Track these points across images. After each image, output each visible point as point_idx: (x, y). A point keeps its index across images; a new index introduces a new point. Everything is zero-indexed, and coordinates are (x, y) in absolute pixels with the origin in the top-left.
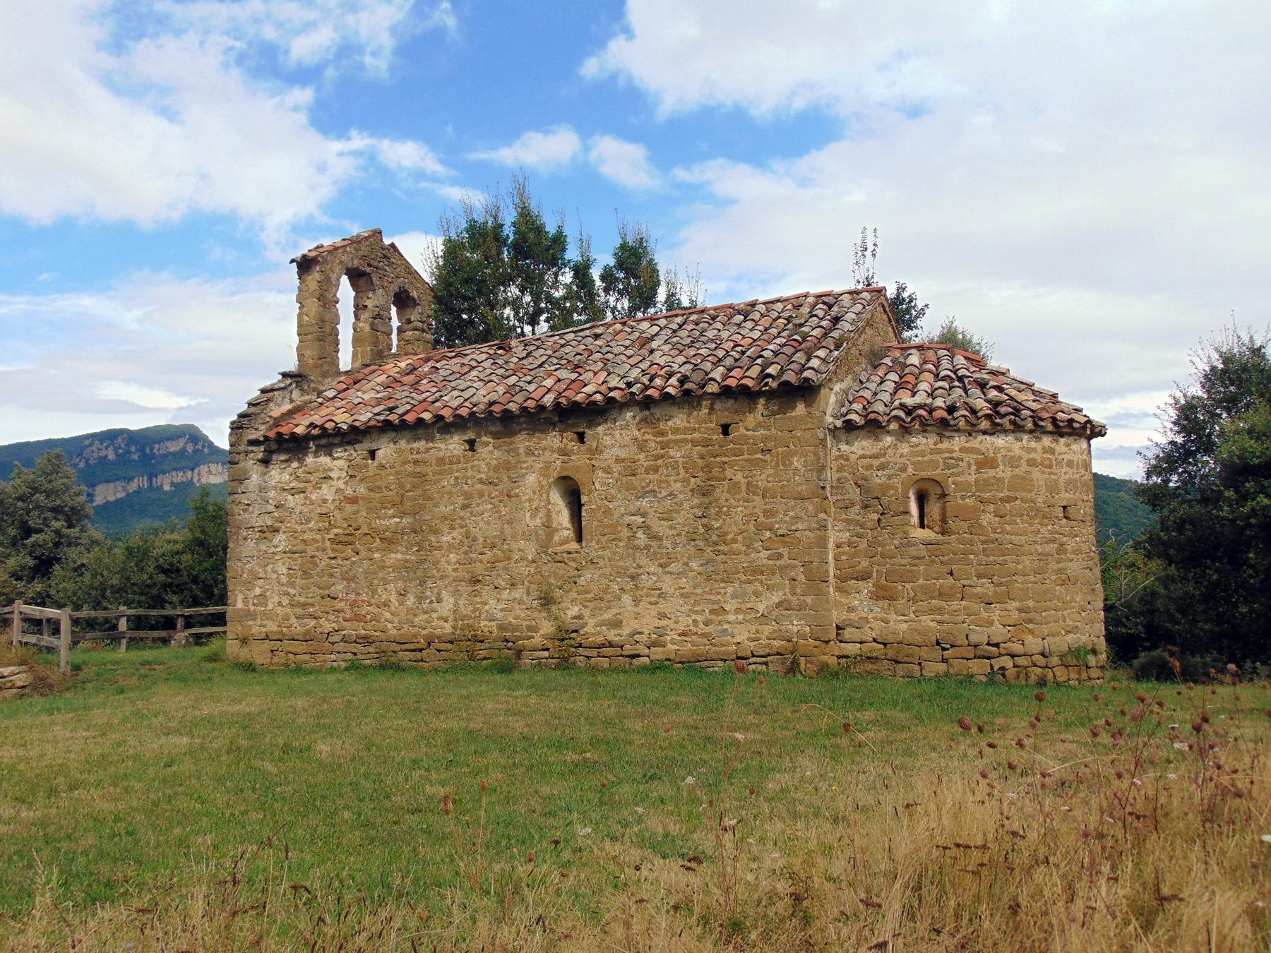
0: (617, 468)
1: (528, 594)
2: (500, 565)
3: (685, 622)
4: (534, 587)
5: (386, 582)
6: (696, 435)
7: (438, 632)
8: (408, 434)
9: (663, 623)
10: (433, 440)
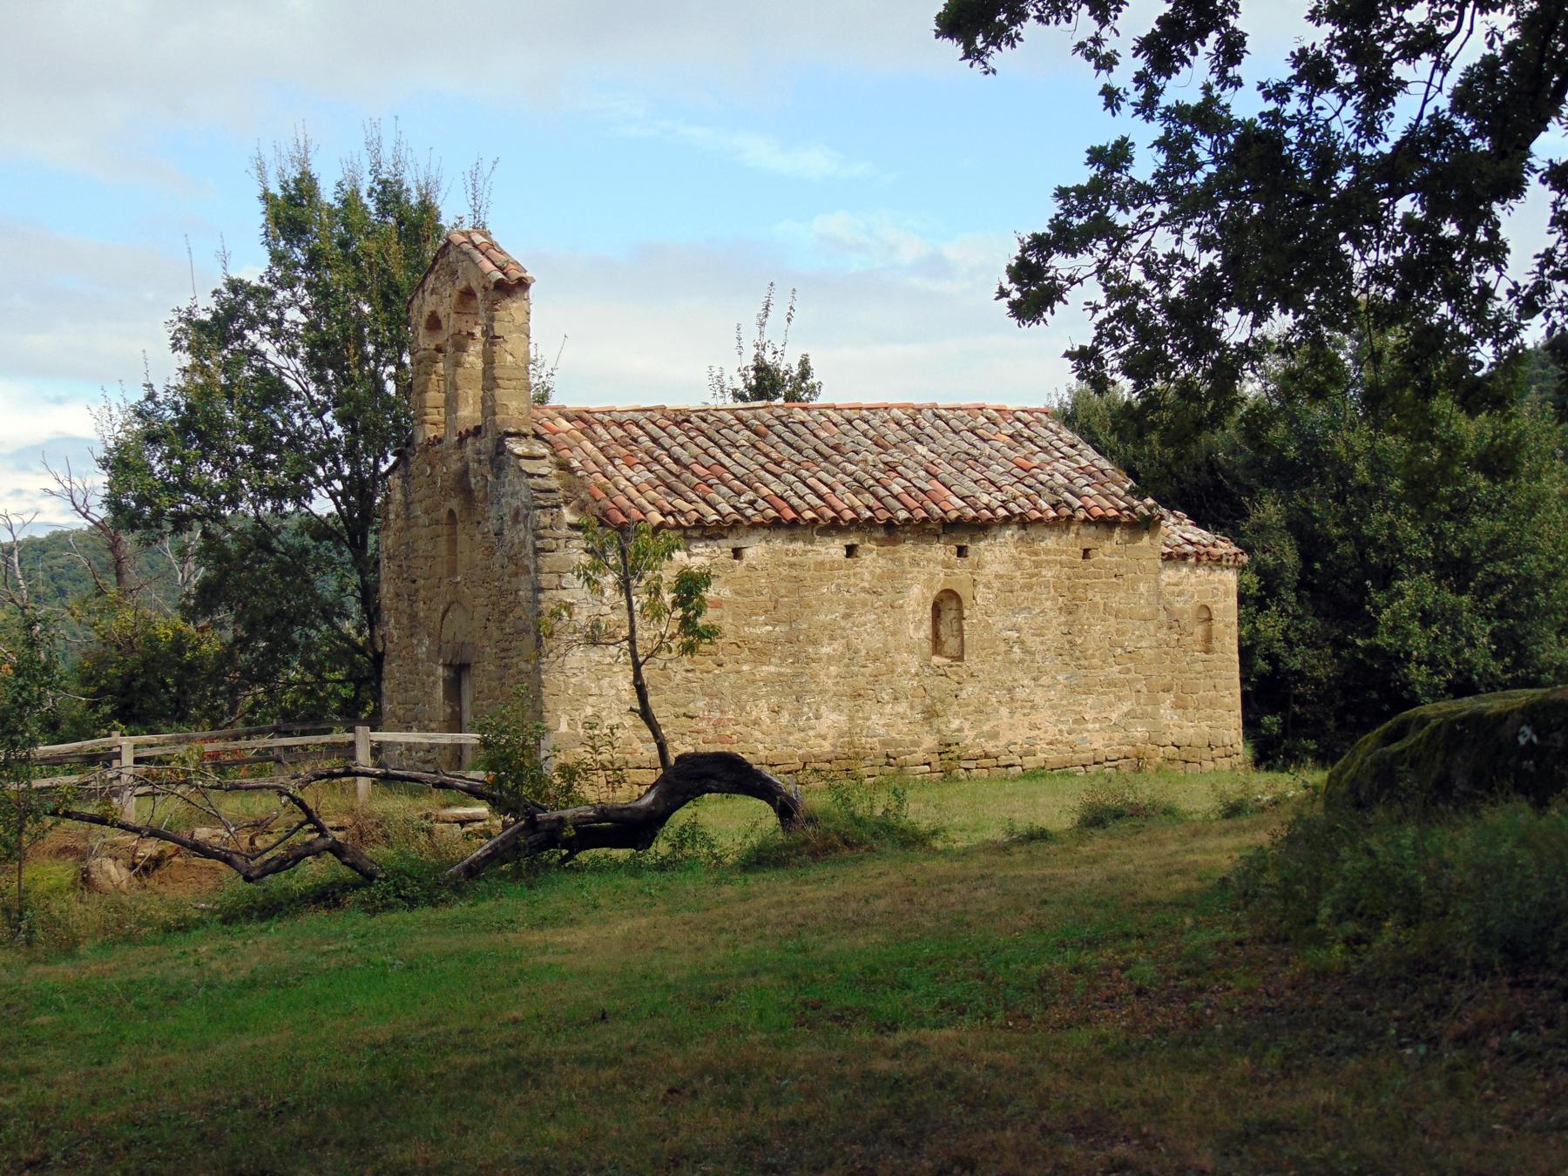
0: (996, 584)
1: (912, 708)
2: (884, 678)
3: (1052, 732)
4: (918, 701)
5: (756, 697)
6: (1064, 557)
7: (816, 751)
8: (784, 533)
9: (1034, 733)
10: (812, 542)
